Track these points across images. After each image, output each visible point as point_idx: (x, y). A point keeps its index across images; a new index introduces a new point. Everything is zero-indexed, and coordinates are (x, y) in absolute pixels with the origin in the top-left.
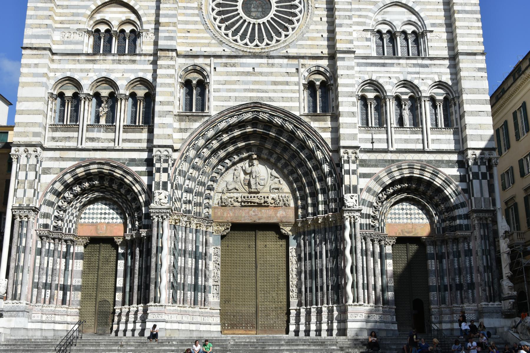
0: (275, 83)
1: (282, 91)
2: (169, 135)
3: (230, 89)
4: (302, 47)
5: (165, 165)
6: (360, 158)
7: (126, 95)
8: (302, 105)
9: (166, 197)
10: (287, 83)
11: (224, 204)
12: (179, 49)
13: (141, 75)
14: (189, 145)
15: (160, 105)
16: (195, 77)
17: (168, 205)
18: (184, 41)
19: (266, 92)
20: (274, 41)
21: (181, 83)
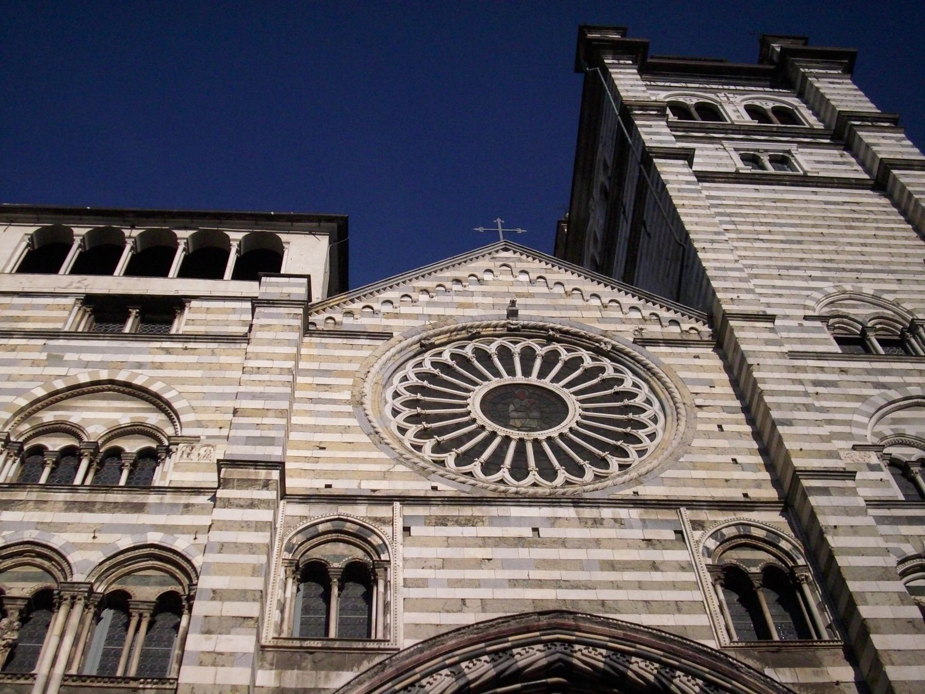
0: (611, 565)
1: (640, 585)
4: (678, 482)
7: (91, 591)
10: (654, 566)
12: (289, 483)
13: (154, 538)
15: (213, 599)
16: (338, 555)
18: (308, 466)
19: (587, 587)
20: (589, 476)
21: (291, 562)
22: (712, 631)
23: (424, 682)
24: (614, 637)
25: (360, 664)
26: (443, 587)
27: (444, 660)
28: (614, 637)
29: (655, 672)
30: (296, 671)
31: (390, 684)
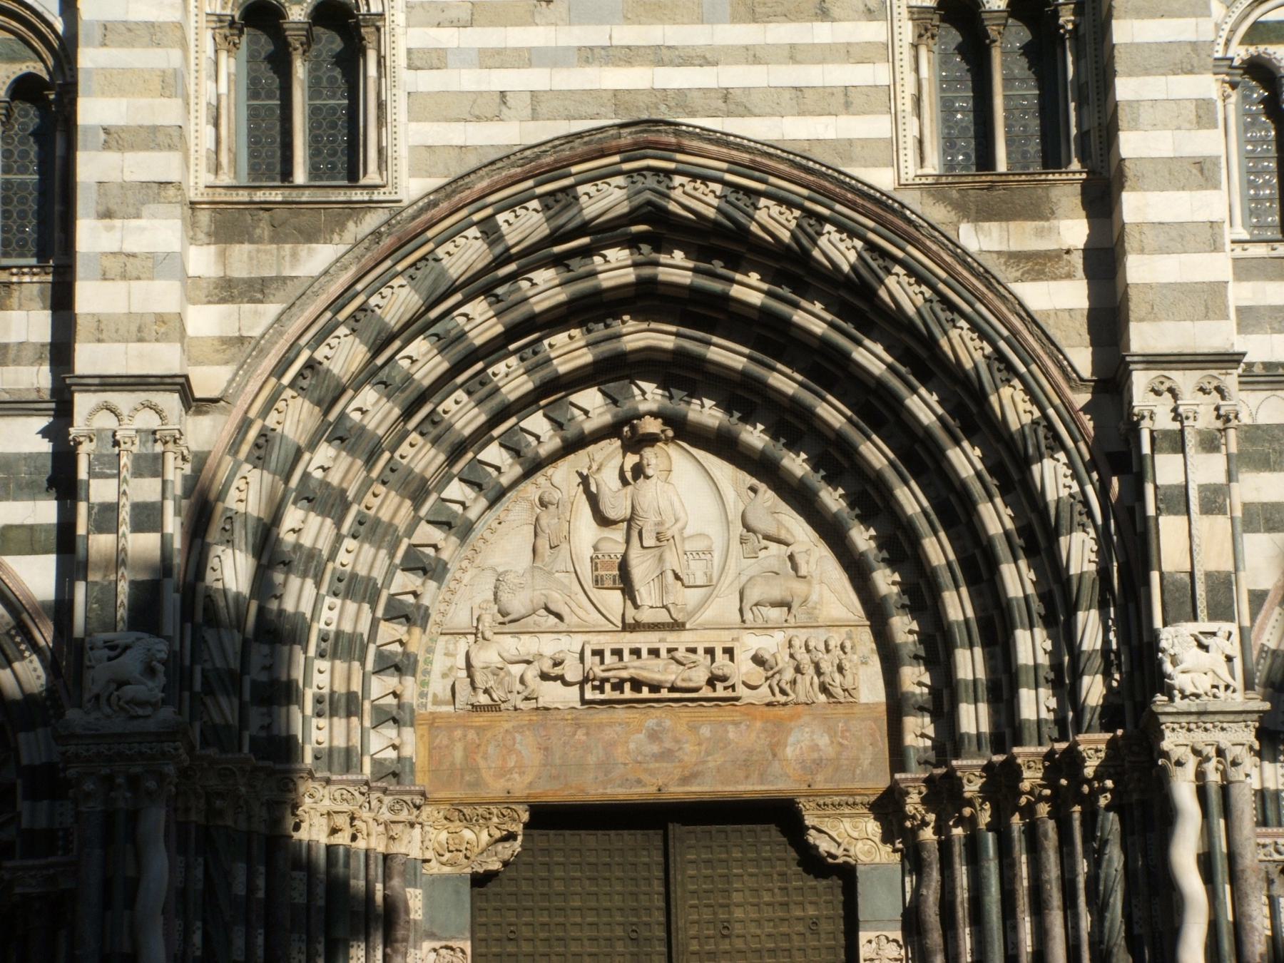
1: (794, 54)
2: (161, 318)
3: (499, 52)
5: (147, 490)
6: (1245, 419)
8: (911, 128)
9: (150, 671)
11: (483, 699)
14: (279, 370)
15: (106, 146)
17: (167, 713)
21: (220, 19)
22: (889, 151)
23: (440, 252)
24: (737, 167)
25: (343, 227)
26: (470, 66)
27: (471, 214)
28: (737, 167)
29: (793, 224)
30: (246, 247)
31: (388, 263)
